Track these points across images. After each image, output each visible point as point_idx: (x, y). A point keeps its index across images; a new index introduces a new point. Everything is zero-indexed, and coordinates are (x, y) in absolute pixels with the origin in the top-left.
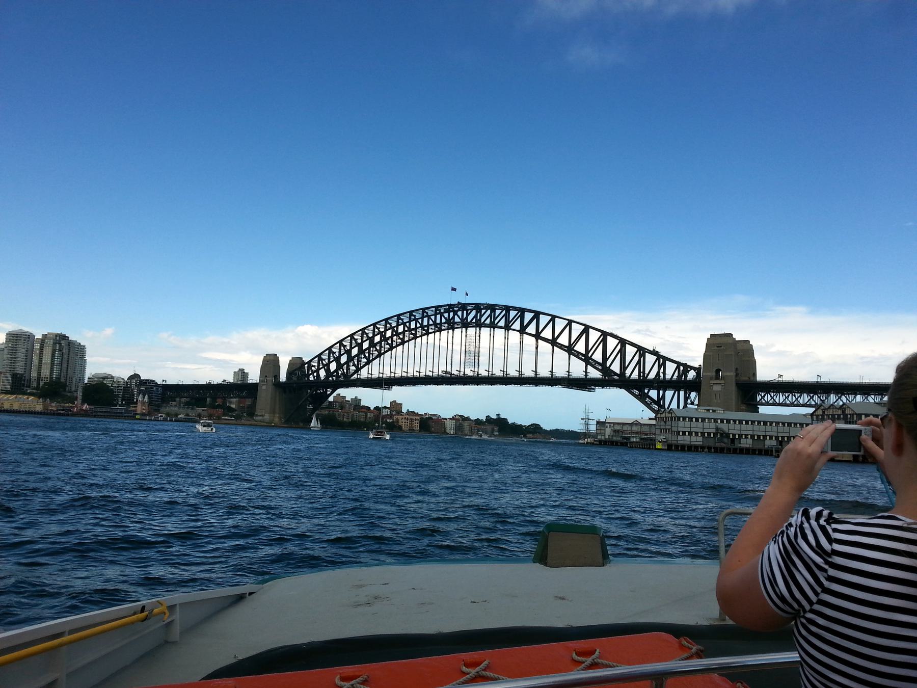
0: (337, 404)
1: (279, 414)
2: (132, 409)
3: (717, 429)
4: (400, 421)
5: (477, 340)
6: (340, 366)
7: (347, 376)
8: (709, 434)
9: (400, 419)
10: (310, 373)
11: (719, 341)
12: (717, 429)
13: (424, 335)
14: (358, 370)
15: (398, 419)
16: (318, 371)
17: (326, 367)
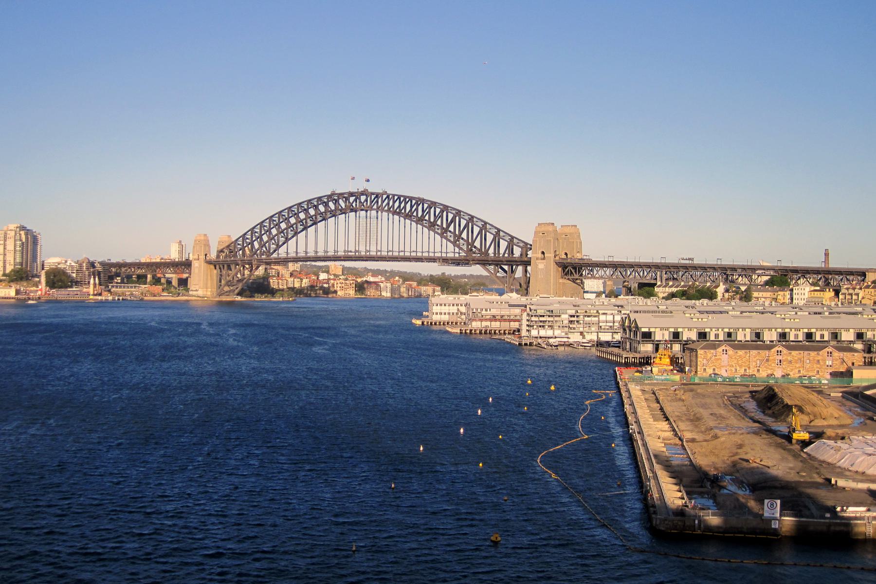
0: (274, 271)
1: (211, 288)
2: (85, 290)
3: (458, 310)
4: (335, 286)
5: (368, 227)
6: (262, 245)
7: (269, 253)
8: (453, 314)
9: (335, 284)
10: (245, 245)
11: (543, 229)
12: (458, 310)
13: (330, 217)
14: (278, 247)
15: (333, 285)
16: (243, 249)
17: (250, 246)
